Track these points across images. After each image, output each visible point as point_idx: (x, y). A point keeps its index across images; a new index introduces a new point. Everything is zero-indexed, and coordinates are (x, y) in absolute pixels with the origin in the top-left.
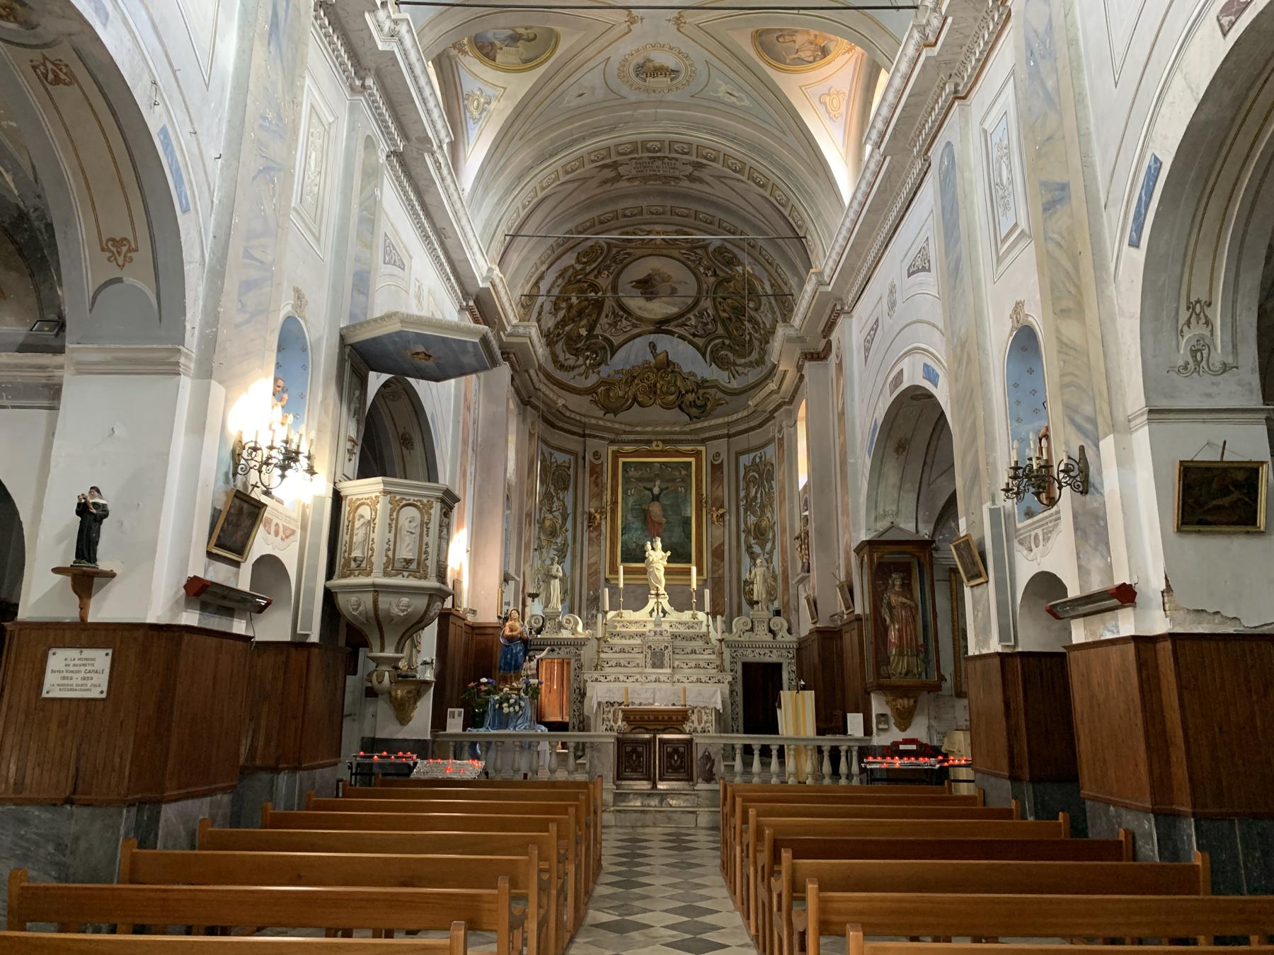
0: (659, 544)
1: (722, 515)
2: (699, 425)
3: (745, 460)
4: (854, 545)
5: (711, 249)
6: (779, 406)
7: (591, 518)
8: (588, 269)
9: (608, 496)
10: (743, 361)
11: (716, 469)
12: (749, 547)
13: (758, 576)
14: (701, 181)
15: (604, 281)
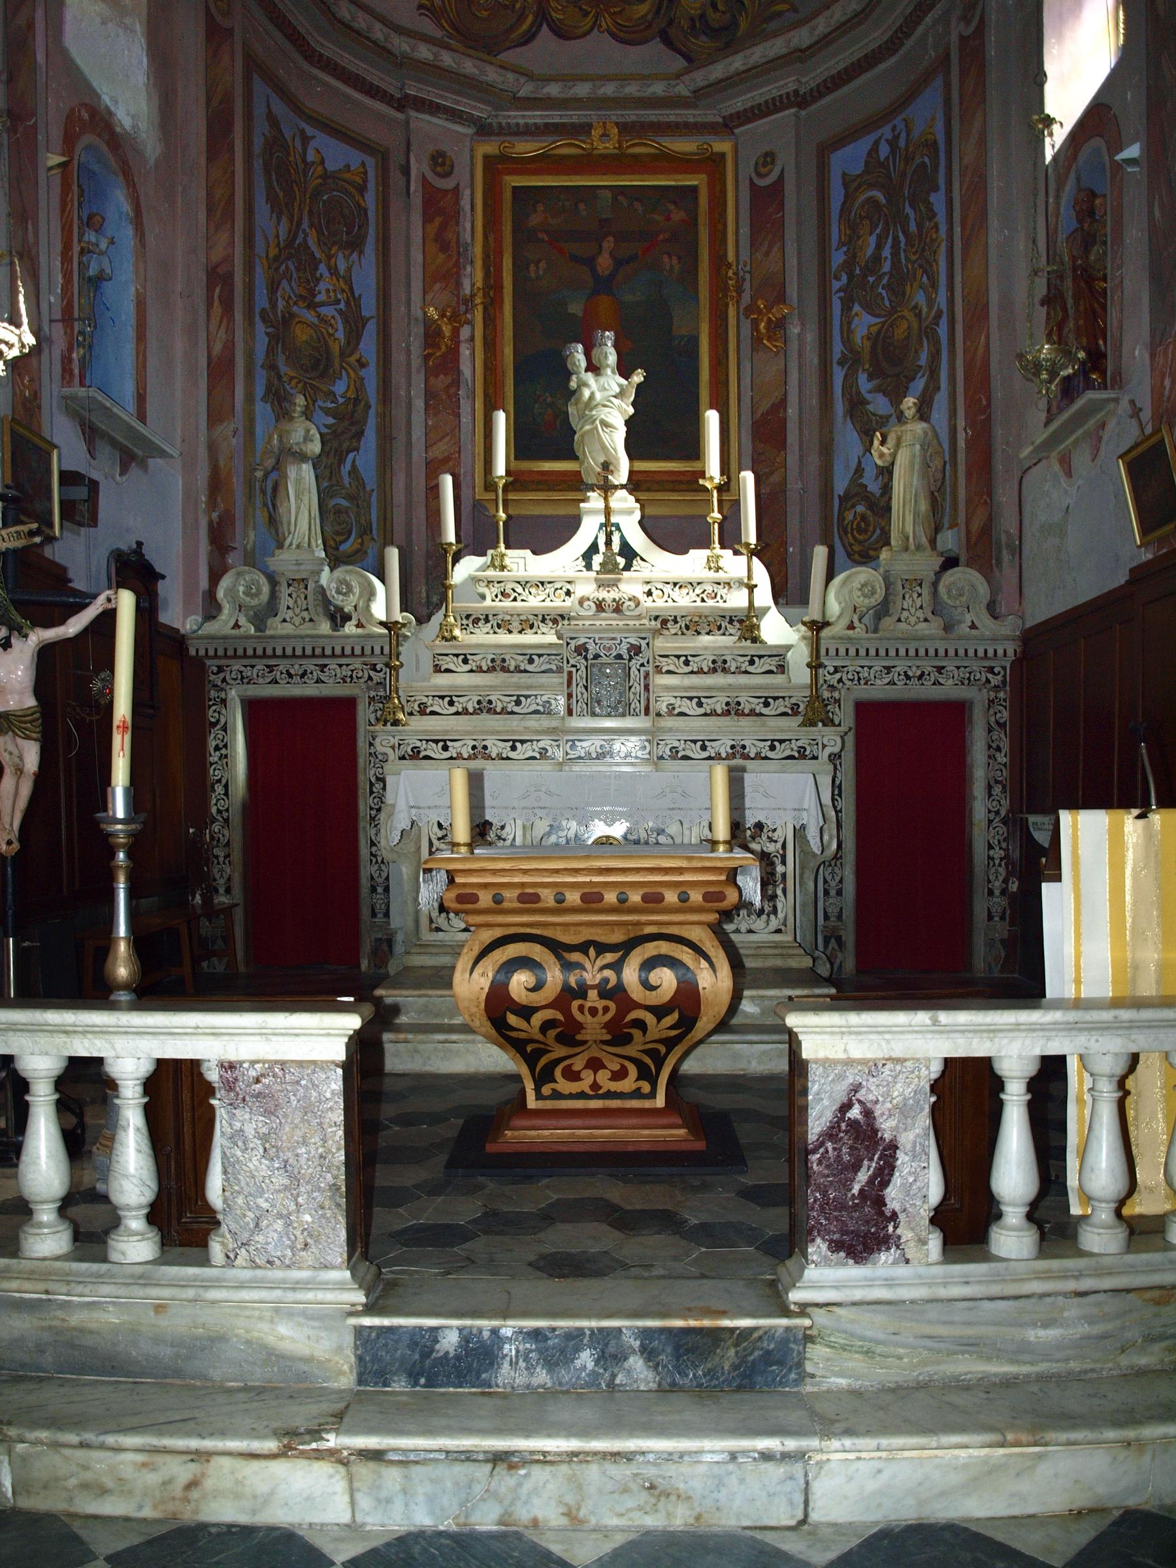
7: (432, 336)
9: (473, 278)
12: (856, 405)
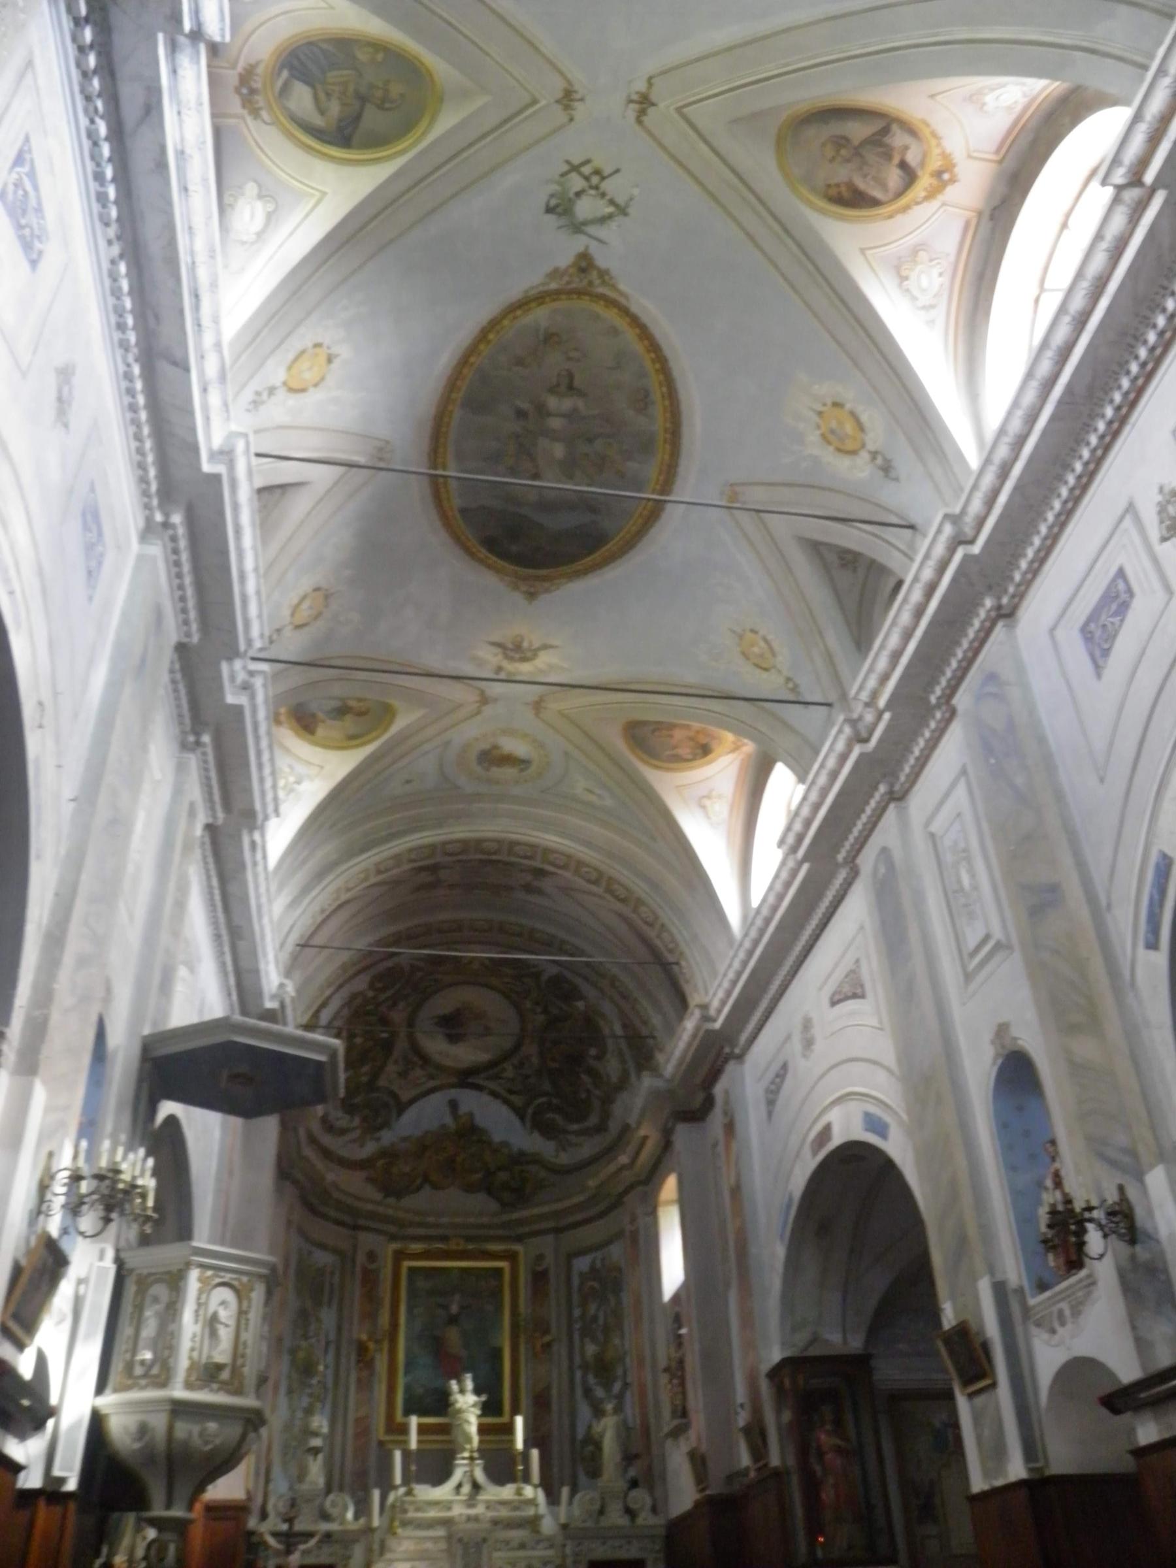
0: (469, 1384)
1: (548, 1345)
2: (516, 1215)
3: (582, 1264)
4: (765, 1368)
5: (545, 977)
6: (626, 1191)
8: (383, 997)
10: (575, 1127)
11: (539, 1278)
12: (588, 1392)
13: (608, 1430)
14: (540, 892)
15: (398, 1016)
